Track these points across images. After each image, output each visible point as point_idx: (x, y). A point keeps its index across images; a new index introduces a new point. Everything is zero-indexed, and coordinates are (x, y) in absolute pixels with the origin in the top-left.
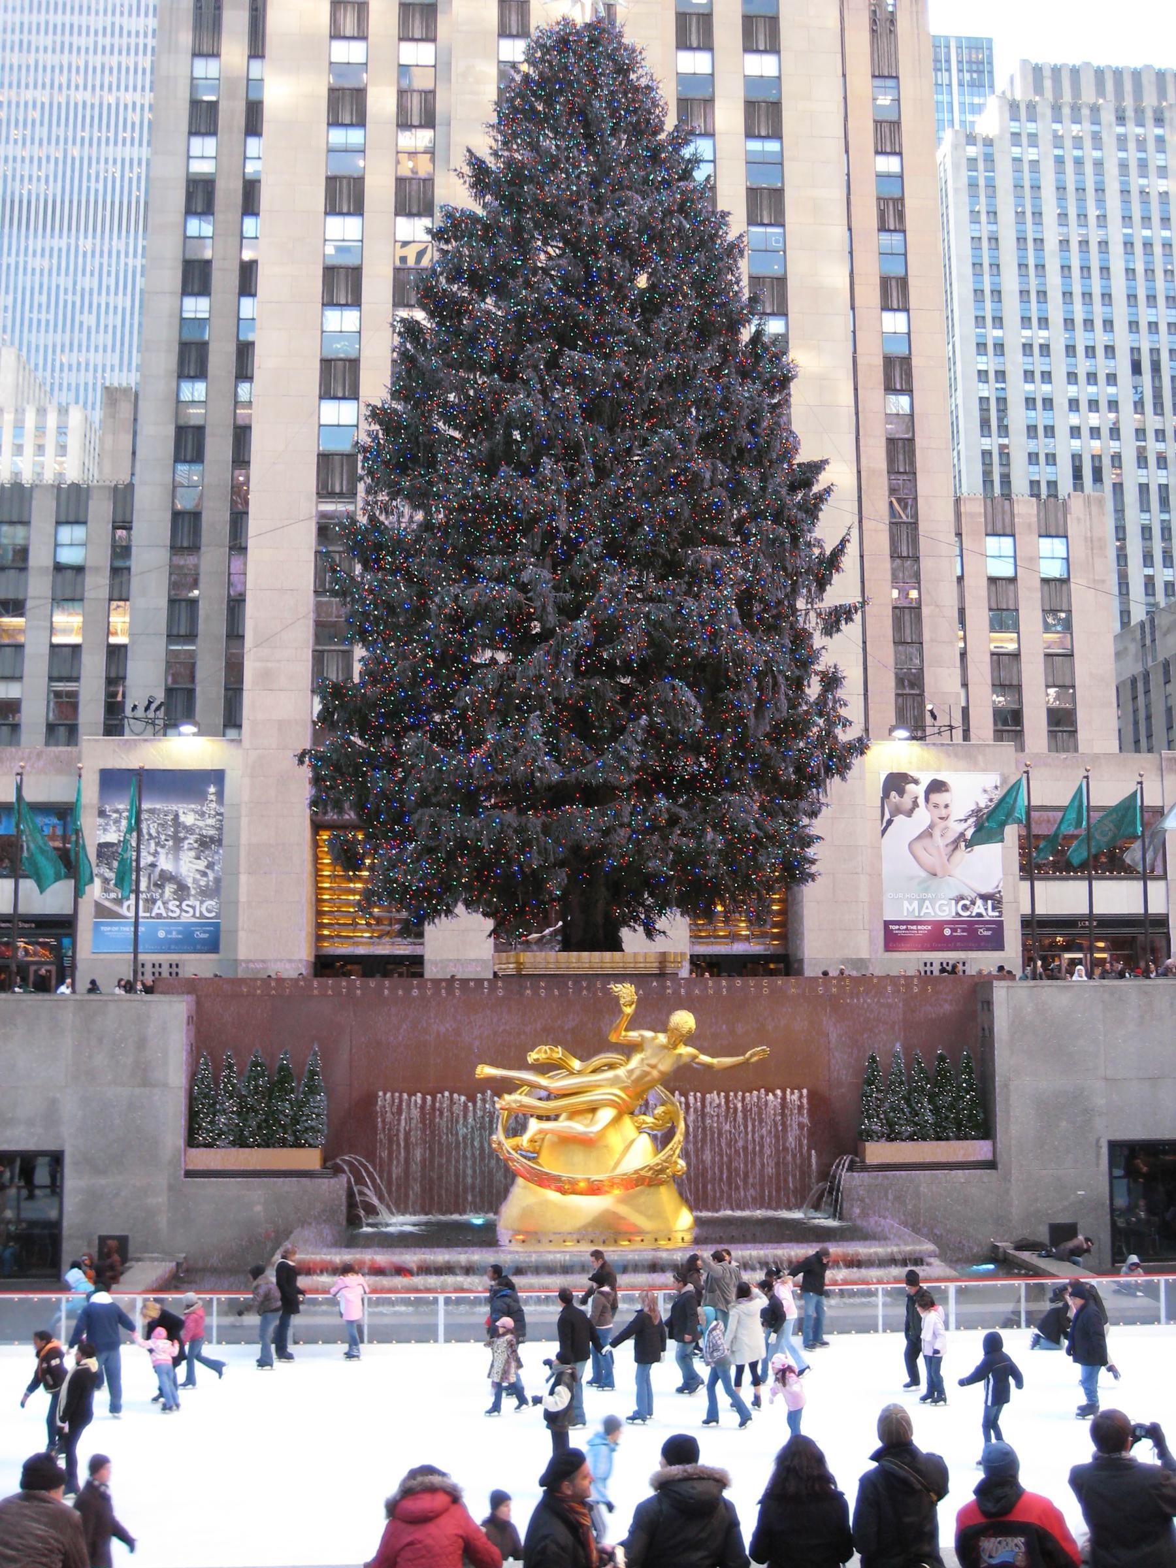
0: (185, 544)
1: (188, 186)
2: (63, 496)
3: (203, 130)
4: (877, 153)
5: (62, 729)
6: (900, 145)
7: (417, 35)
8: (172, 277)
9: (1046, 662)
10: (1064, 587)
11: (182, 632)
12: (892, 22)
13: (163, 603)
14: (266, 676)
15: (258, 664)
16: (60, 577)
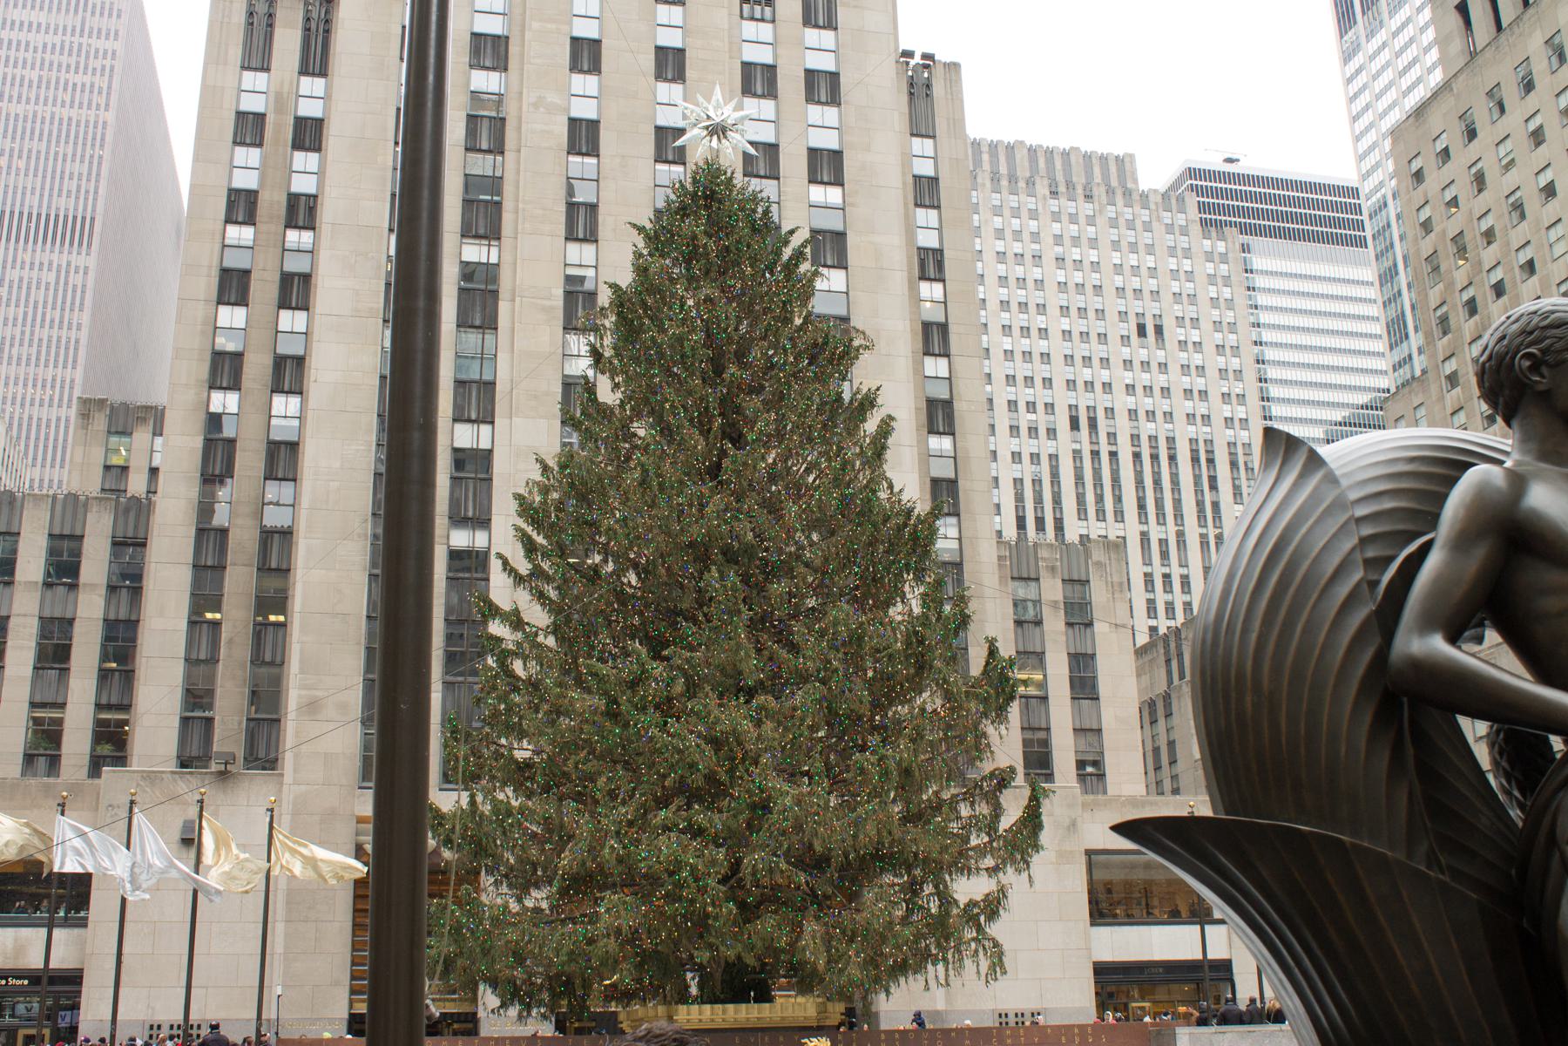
0: (209, 563)
1: (229, 196)
2: (59, 508)
3: (248, 141)
4: (917, 205)
5: (42, 759)
6: (939, 200)
7: (488, 64)
8: (208, 284)
9: (1073, 706)
10: (1088, 630)
11: (202, 656)
12: (928, 86)
13: (183, 625)
14: (312, 707)
15: (304, 692)
16: (49, 593)
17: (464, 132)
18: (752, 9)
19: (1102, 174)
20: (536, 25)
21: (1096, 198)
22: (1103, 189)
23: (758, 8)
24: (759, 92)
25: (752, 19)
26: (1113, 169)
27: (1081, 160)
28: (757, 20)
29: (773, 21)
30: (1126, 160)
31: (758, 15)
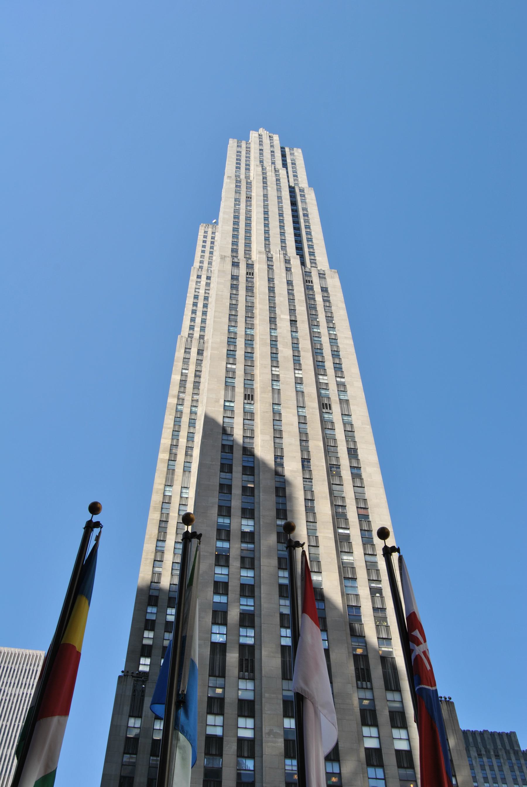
7: (246, 714)
17: (236, 748)
18: (362, 684)
19: (501, 744)
20: (267, 695)
21: (501, 756)
22: (503, 751)
23: (364, 683)
24: (370, 723)
25: (362, 688)
26: (506, 740)
27: (490, 737)
28: (365, 689)
29: (372, 689)
30: (512, 736)
31: (365, 686)
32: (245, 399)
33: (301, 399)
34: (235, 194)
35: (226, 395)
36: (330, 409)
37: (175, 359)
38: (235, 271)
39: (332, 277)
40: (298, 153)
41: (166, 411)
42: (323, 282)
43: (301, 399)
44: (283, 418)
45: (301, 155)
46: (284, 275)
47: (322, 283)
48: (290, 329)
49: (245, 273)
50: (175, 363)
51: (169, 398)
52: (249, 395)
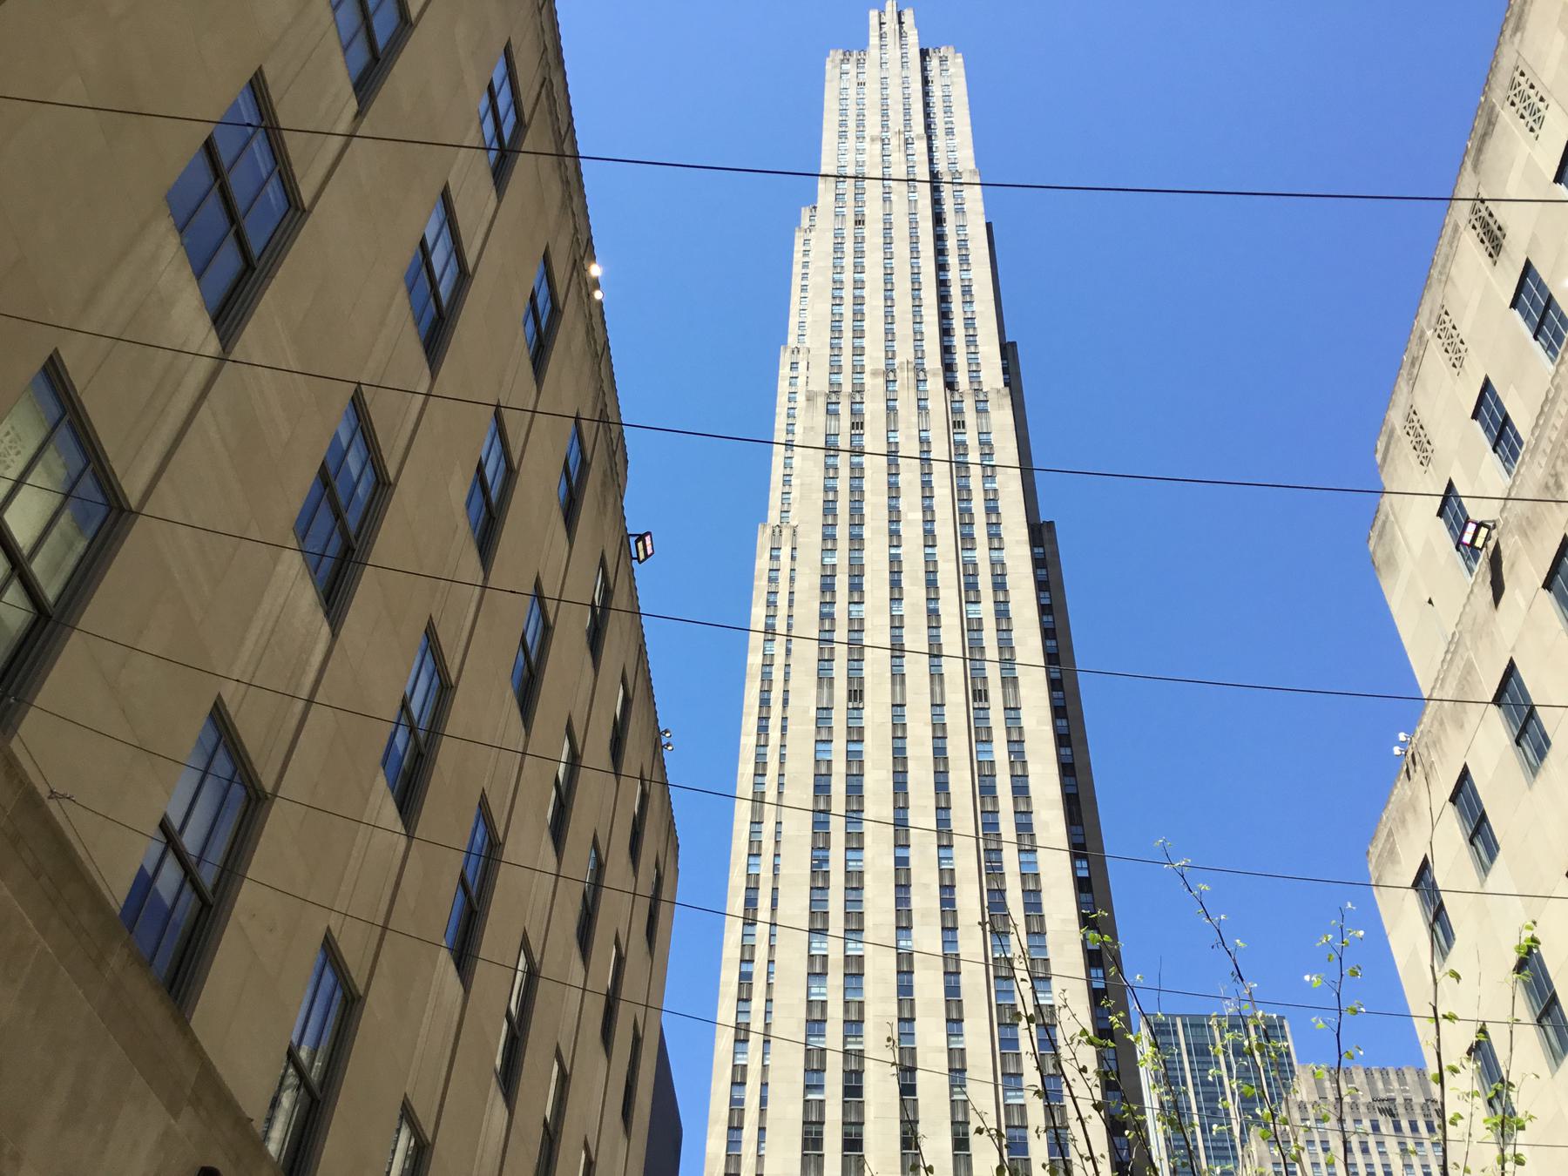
32: (850, 700)
33: (937, 689)
34: (835, 219)
35: (819, 698)
36: (986, 700)
37: (756, 574)
38: (833, 423)
39: (1000, 407)
40: (956, 65)
41: (747, 680)
42: (984, 421)
43: (937, 689)
44: (909, 733)
45: (962, 71)
46: (915, 419)
47: (982, 423)
48: (922, 543)
49: (849, 425)
50: (756, 583)
51: (749, 654)
52: (856, 691)
